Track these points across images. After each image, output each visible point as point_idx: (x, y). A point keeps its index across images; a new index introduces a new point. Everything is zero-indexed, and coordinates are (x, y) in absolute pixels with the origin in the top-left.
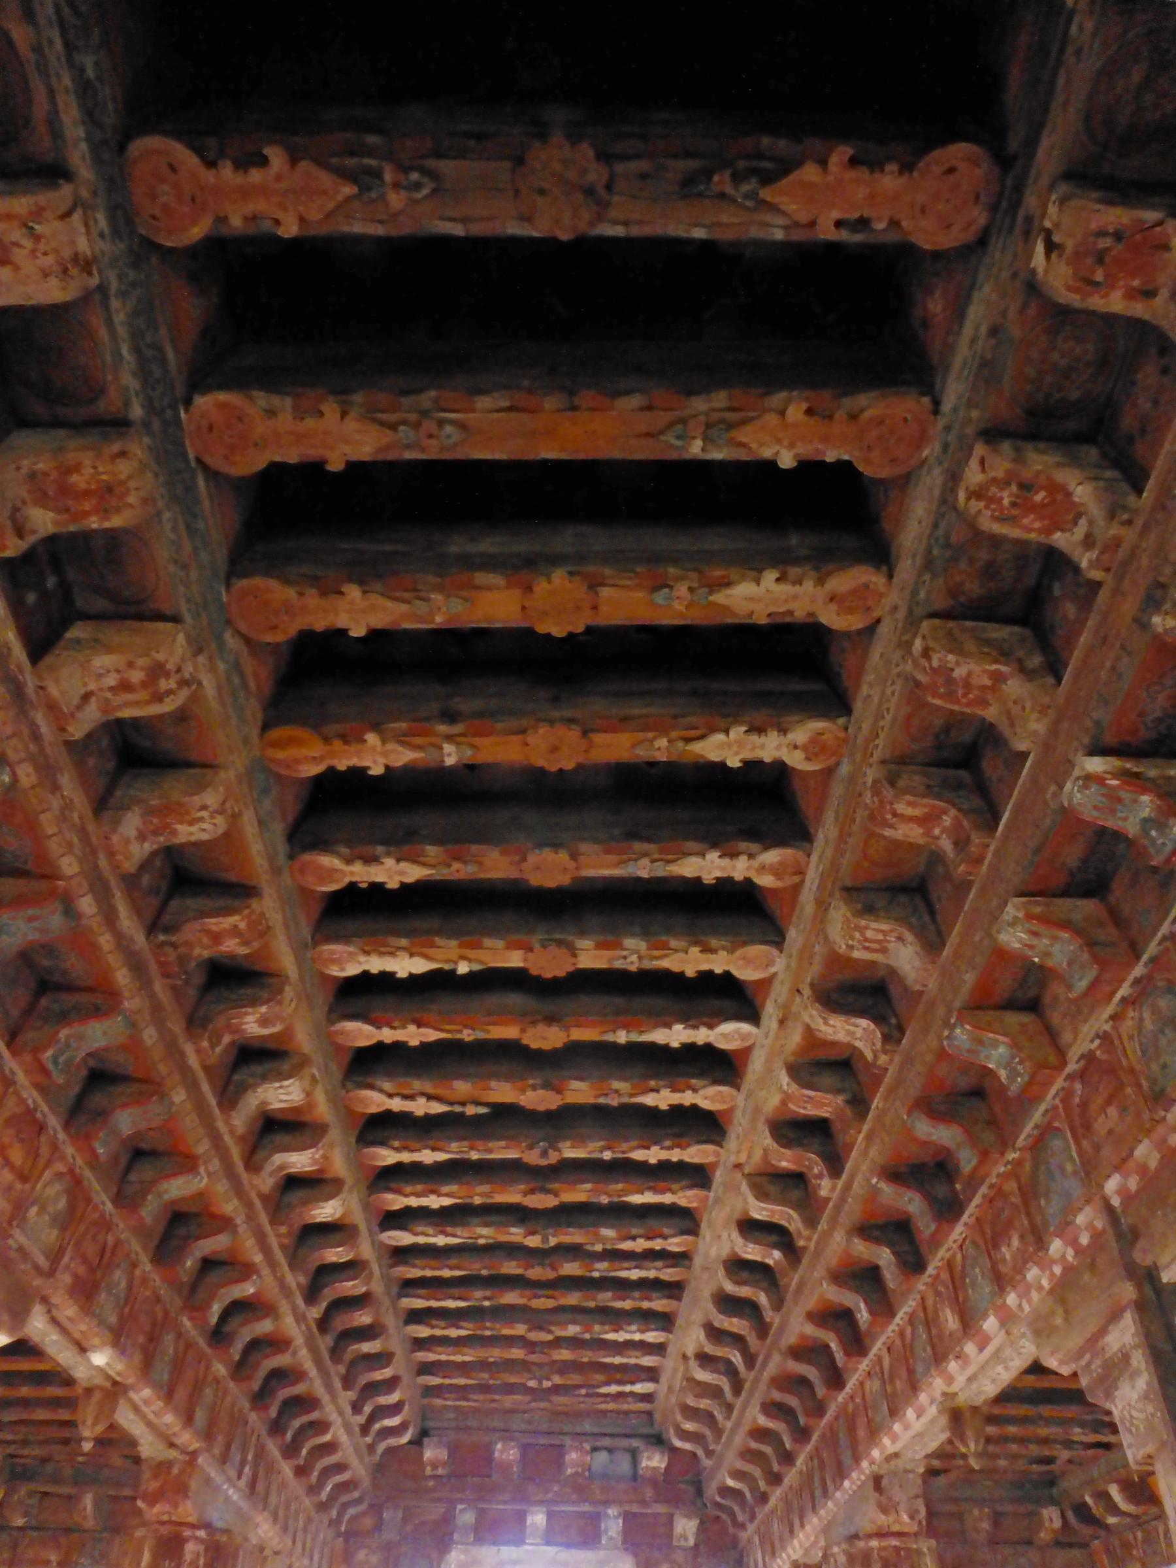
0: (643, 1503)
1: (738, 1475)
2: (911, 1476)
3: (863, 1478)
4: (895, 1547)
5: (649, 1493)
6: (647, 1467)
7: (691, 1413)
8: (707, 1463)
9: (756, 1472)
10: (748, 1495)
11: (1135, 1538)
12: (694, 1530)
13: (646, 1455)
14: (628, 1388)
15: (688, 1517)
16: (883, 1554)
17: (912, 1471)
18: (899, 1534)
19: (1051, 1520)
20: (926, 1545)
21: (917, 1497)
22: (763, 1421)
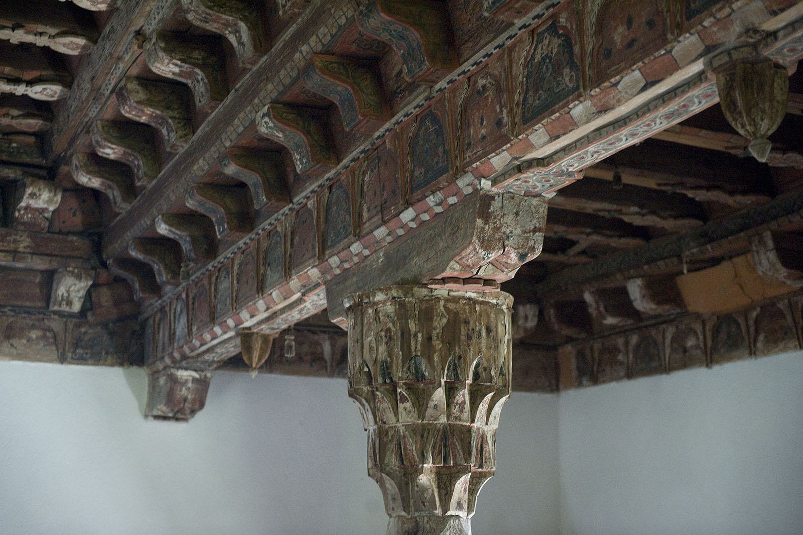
0: (15, 253)
1: (184, 218)
2: (535, 202)
3: (452, 200)
4: (470, 299)
5: (24, 243)
6: (27, 208)
7: (124, 129)
8: (123, 207)
9: (217, 212)
10: (186, 246)
11: (627, 343)
12: (82, 293)
13: (29, 191)
14: (20, 90)
15: (79, 277)
16: (451, 306)
17: (538, 195)
18: (488, 282)
19: (526, 318)
20: (506, 301)
21: (535, 230)
22: (266, 127)
